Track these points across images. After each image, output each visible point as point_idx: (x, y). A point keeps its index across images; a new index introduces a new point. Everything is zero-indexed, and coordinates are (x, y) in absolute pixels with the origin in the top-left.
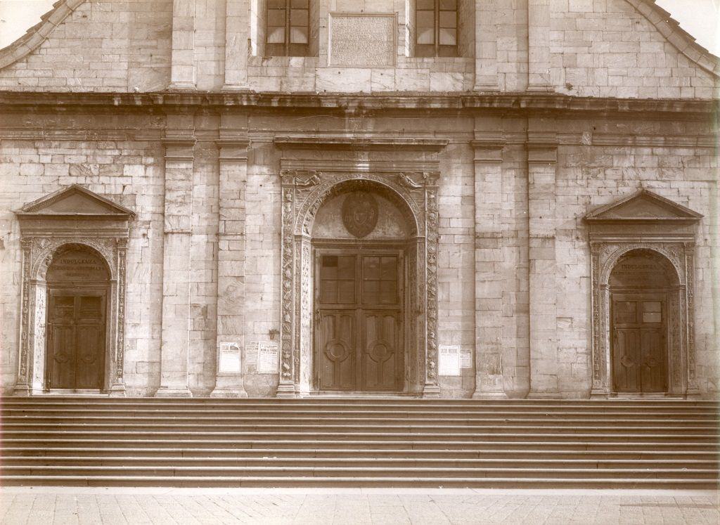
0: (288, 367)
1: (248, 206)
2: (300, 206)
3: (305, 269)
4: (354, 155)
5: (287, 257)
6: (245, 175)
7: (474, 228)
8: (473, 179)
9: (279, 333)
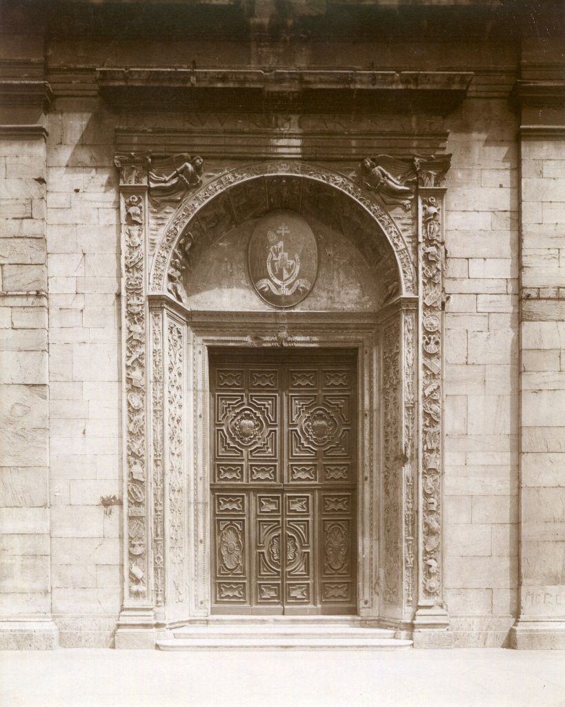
0: (140, 574)
1: (52, 235)
2: (160, 236)
3: (175, 372)
4: (270, 122)
5: (135, 342)
6: (43, 167)
7: (519, 279)
8: (515, 173)
9: (121, 503)
